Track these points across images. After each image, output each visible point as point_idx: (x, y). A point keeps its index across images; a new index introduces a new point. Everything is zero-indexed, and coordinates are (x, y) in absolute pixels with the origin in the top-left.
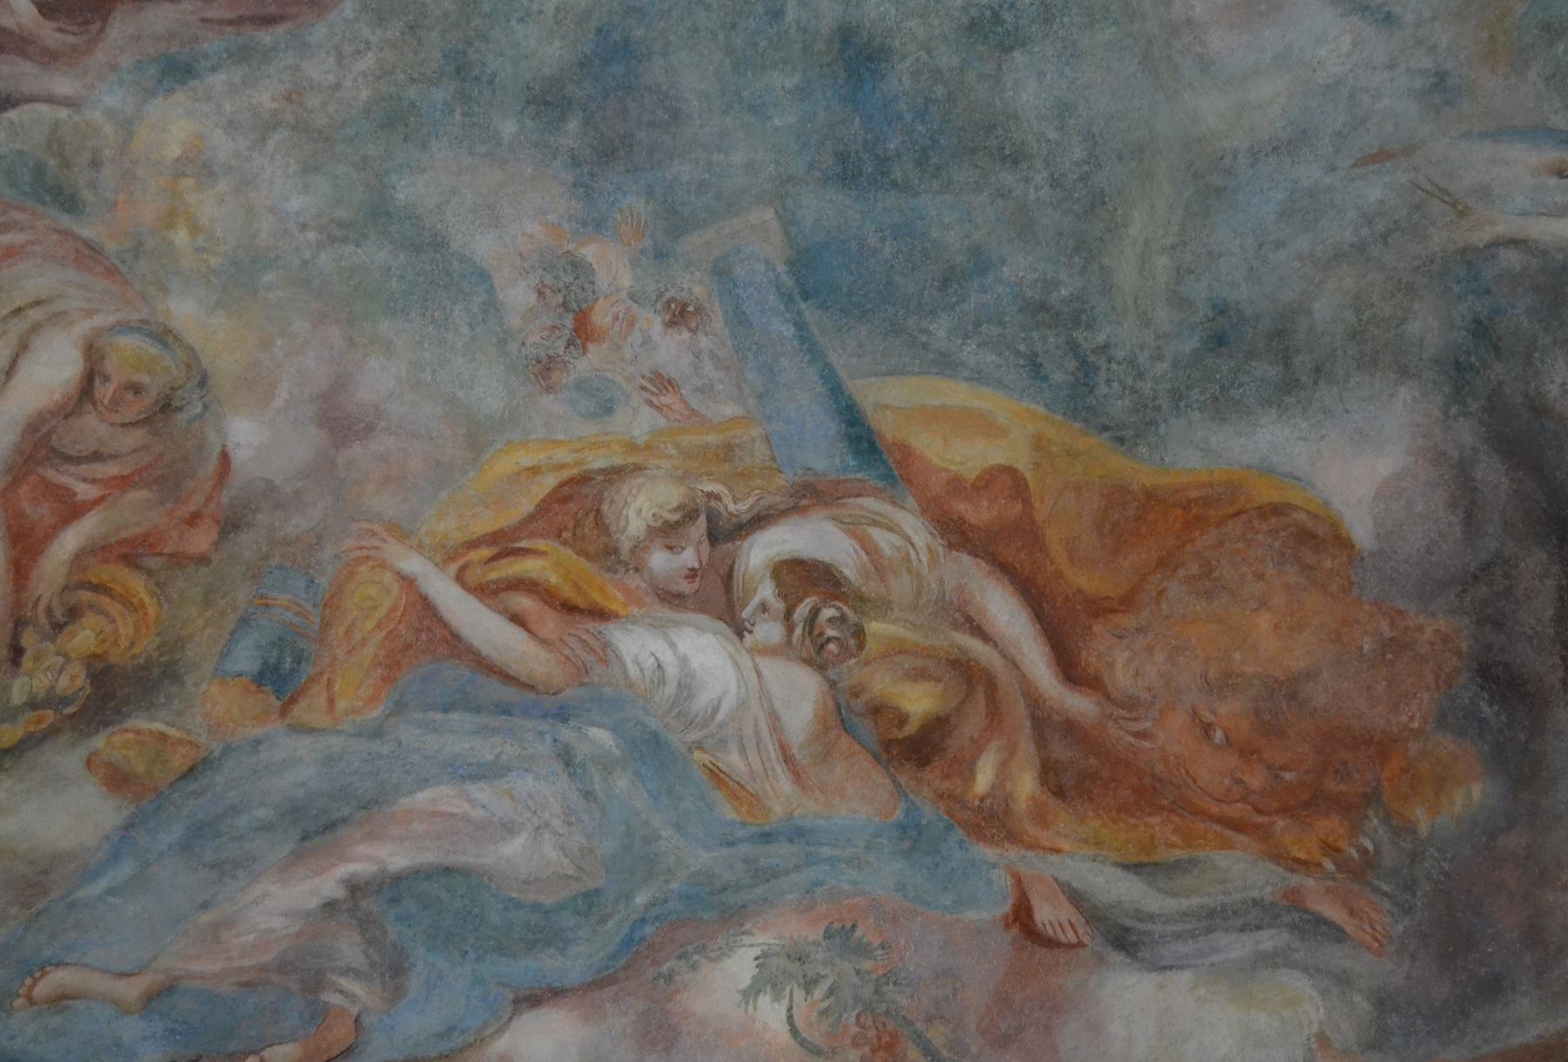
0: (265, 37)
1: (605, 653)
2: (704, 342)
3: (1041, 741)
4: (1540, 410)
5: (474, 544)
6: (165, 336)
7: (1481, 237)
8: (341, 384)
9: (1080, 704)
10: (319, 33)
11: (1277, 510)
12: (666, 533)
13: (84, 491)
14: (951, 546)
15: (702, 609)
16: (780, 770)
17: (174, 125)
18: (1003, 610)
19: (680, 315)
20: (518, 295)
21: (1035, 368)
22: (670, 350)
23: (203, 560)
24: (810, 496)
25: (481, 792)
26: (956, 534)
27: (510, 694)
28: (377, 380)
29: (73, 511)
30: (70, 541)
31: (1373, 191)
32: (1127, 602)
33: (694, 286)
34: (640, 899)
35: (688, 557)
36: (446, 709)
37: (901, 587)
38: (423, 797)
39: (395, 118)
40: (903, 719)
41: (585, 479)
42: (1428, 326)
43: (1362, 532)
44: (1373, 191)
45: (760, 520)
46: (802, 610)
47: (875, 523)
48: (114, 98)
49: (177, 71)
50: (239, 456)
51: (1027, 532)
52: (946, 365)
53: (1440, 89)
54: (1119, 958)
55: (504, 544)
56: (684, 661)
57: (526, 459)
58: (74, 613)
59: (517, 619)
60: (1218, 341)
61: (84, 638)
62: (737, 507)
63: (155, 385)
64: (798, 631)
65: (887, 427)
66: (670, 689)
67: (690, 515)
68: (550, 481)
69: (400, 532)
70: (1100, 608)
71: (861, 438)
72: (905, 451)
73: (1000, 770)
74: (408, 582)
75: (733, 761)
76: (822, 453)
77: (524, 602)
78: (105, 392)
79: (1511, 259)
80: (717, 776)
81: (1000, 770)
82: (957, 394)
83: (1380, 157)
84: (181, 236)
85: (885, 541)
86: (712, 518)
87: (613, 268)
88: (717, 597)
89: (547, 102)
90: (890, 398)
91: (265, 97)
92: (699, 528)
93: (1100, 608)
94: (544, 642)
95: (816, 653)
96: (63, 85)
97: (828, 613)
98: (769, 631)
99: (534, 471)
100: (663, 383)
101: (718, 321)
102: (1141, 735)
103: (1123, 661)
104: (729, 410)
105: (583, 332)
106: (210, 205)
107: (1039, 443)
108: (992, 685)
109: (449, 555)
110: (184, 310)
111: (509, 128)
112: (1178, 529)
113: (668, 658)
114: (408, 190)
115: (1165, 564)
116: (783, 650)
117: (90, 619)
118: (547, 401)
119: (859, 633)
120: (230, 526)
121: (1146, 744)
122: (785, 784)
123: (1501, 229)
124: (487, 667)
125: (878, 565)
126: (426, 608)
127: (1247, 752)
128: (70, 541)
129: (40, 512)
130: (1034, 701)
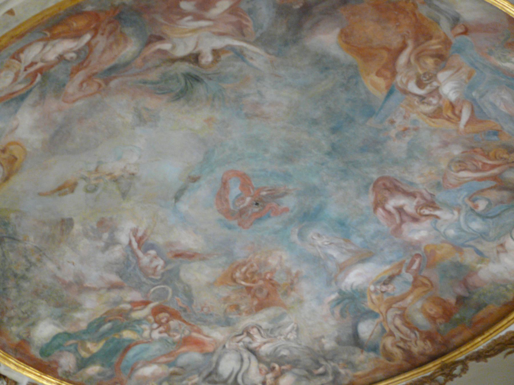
0: (398, 179)
1: (458, 100)
2: (394, 117)
3: (423, 43)
4: (289, 29)
5: (453, 122)
6: (449, 167)
7: (273, 57)
8: (439, 147)
9: (410, 43)
10: (392, 175)
11: (346, 42)
12: (429, 104)
13: (480, 164)
14: (397, 73)
15: (438, 93)
16: (461, 71)
17: (418, 180)
18: (403, 59)
19: (392, 122)
20: (407, 139)
21: (356, 84)
22: (399, 120)
23: (481, 148)
24: (405, 92)
25: (498, 104)
26: (394, 74)
27: (476, 107)
28: (435, 144)
29: (484, 164)
30: (490, 162)
31: (282, 72)
32: (385, 48)
33: (386, 124)
34: (503, 79)
35: (431, 99)
36: (485, 113)
37: (411, 73)
38: (504, 110)
39: (396, 162)
40: (435, 61)
41: (429, 117)
42: (294, 50)
43: (337, 31)
44: (282, 72)
45: (416, 95)
46: (427, 82)
47: (403, 83)
48: (421, 187)
49: (412, 184)
50: (461, 151)
51: (385, 67)
52: (368, 93)
53: (259, 79)
54: (461, 19)
55: (449, 119)
56: (450, 91)
57: (432, 124)
58: (501, 158)
59: (461, 112)
60: (327, 68)
61: (505, 156)
62: (417, 99)
63: (457, 165)
64: (431, 81)
65: (385, 92)
66: (457, 90)
67: (423, 103)
68: (433, 120)
69: (457, 130)
70: (388, 50)
71: (390, 92)
72: (387, 87)
73: (434, 45)
74: (465, 126)
75: (464, 77)
76: (398, 95)
77: (457, 112)
78: (463, 168)
79: (271, 51)
80: (469, 78)
81: (434, 45)
82: (371, 88)
83: (276, 76)
84: (433, 171)
85: (404, 80)
86: (421, 101)
87: (393, 132)
88: (435, 92)
89: (377, 152)
90: (380, 95)
91: (406, 175)
92: (426, 101)
93: (388, 50)
94: (462, 107)
95: (433, 77)
96: (424, 191)
97: (424, 79)
98: (435, 84)
99: (433, 122)
100: (405, 117)
101: (389, 118)
102: (408, 32)
103: (396, 42)
104: (401, 109)
105: (406, 129)
106: (426, 171)
107: (368, 74)
108: (418, 54)
109: (457, 123)
110: (443, 166)
111: (385, 153)
112: (365, 52)
113: (452, 92)
114: (404, 156)
115: (372, 48)
116: (436, 80)
117: (501, 156)
118: (421, 126)
119: (425, 74)
120: (473, 148)
121: (410, 31)
122: (463, 69)
123: (268, 56)
124: (473, 111)
125: (409, 79)
126: (468, 123)
127: (397, 20)
128: (490, 162)
129: (488, 167)
130: (415, 48)
